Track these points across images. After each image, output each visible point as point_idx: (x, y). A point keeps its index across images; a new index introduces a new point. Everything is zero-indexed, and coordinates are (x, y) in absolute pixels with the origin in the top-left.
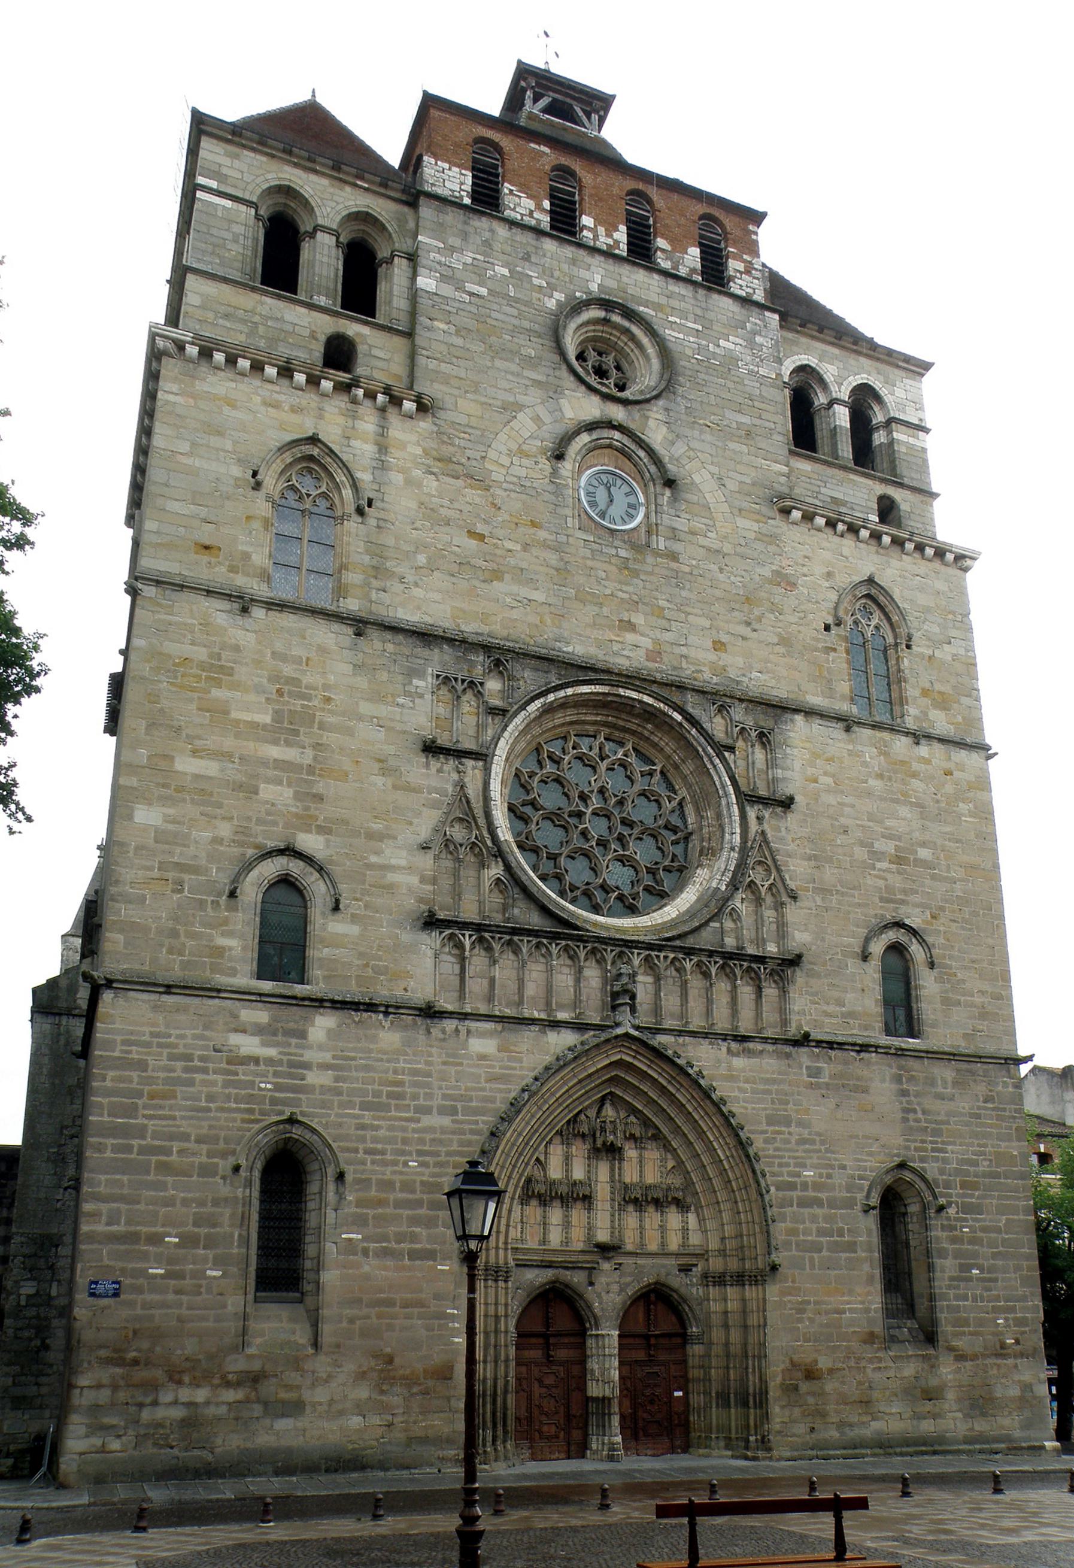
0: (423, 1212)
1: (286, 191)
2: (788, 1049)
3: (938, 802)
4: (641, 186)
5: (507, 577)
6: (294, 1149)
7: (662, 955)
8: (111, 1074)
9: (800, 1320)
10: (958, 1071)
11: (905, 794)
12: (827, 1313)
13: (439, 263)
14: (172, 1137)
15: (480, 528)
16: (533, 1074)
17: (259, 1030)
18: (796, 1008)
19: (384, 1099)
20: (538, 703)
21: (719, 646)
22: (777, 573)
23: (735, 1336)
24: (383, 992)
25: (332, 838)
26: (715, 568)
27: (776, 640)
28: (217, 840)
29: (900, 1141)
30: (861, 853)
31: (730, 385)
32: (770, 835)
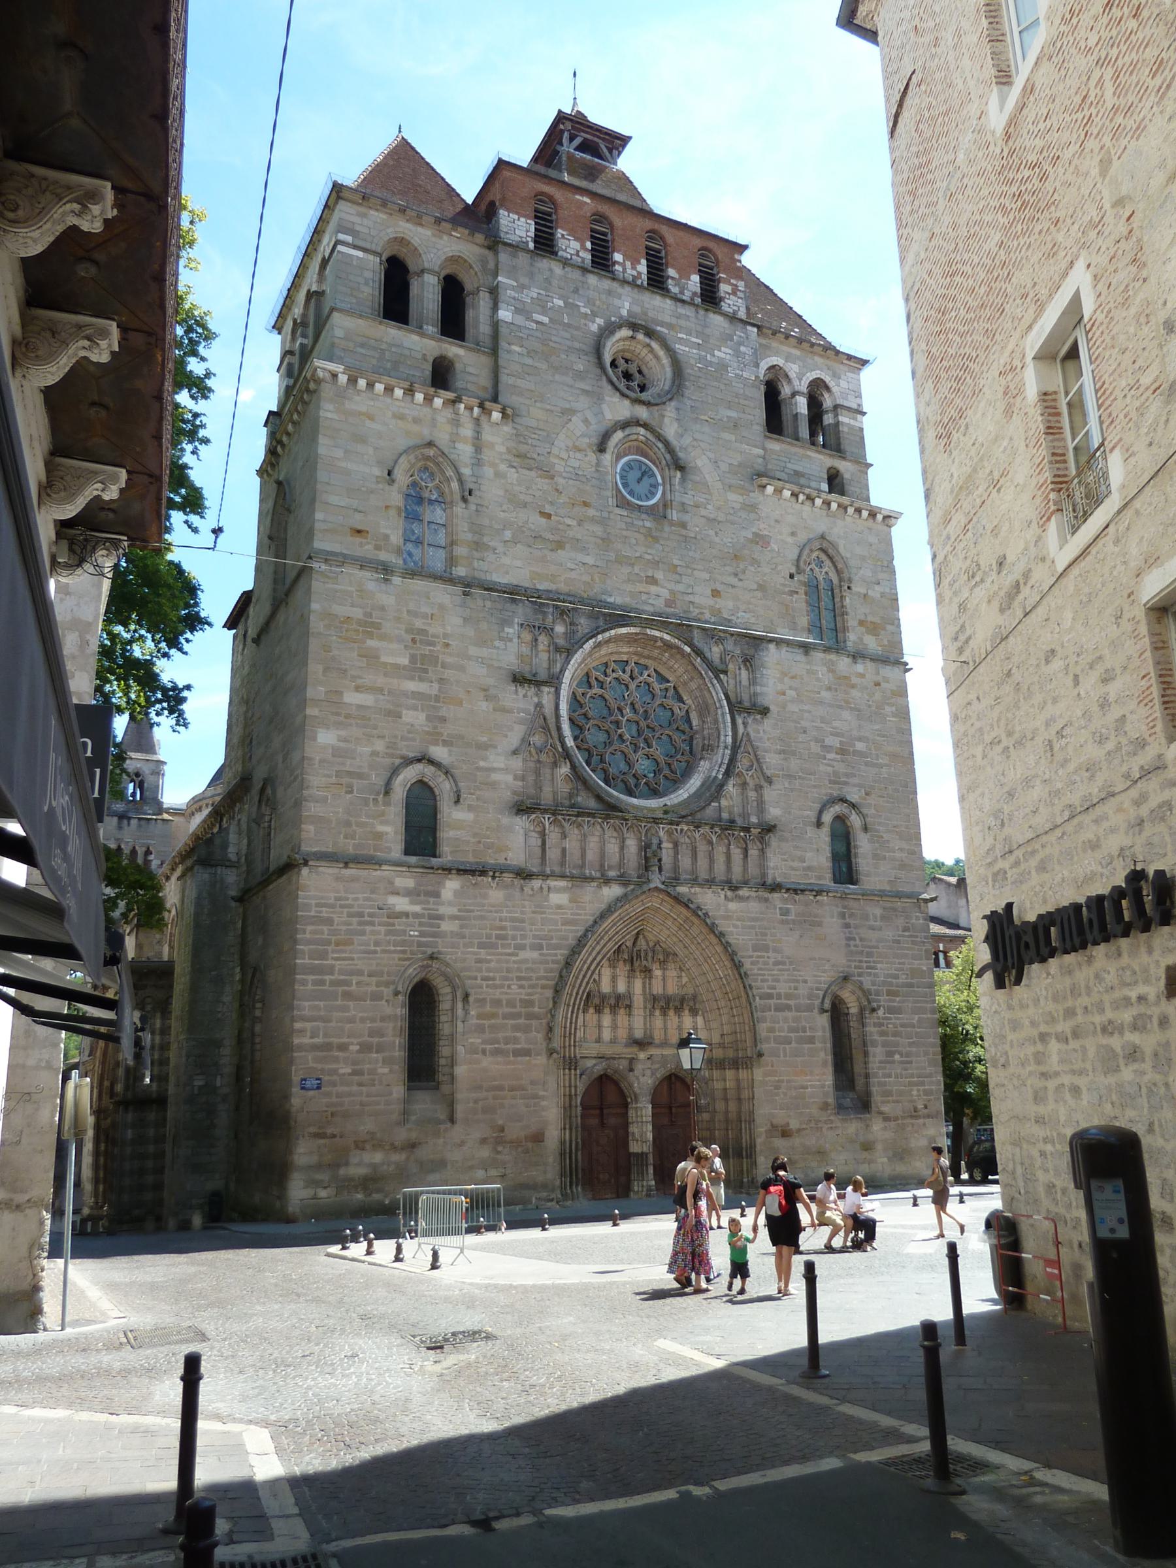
0: (522, 1021)
1: (401, 241)
2: (766, 895)
3: (870, 706)
4: (656, 226)
5: (568, 546)
6: (432, 978)
7: (679, 828)
8: (309, 928)
9: (777, 1094)
10: (884, 908)
11: (847, 702)
12: (795, 1088)
13: (514, 298)
14: (352, 973)
15: (548, 509)
16: (592, 918)
17: (408, 893)
18: (771, 864)
19: (493, 940)
20: (591, 642)
21: (716, 593)
22: (756, 534)
23: (732, 1106)
24: (491, 859)
25: (454, 749)
26: (712, 533)
27: (755, 587)
28: (374, 754)
30: (815, 748)
31: (723, 387)
32: (752, 734)
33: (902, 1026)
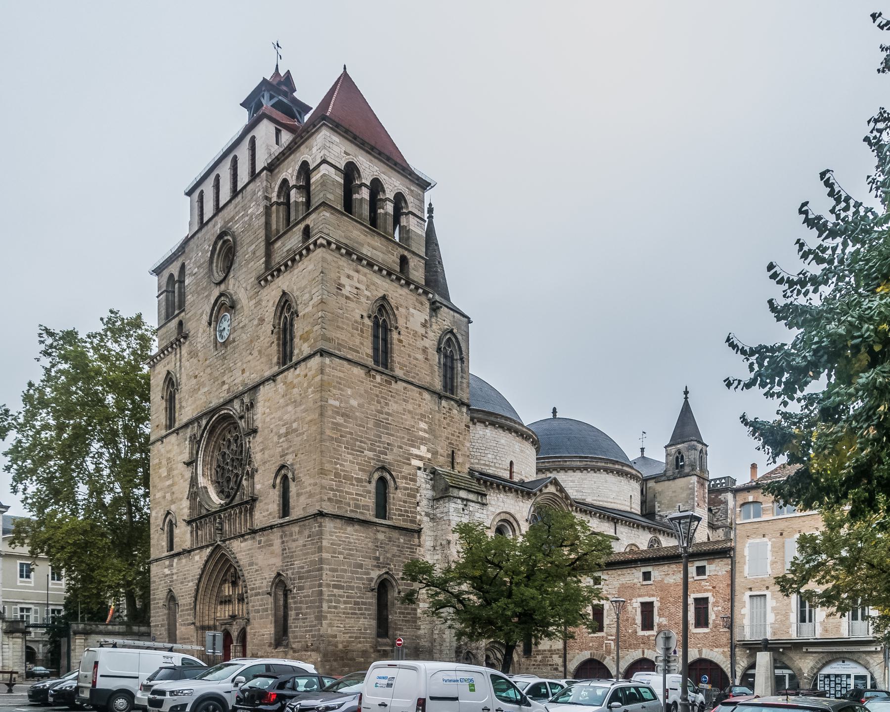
29: (281, 564)
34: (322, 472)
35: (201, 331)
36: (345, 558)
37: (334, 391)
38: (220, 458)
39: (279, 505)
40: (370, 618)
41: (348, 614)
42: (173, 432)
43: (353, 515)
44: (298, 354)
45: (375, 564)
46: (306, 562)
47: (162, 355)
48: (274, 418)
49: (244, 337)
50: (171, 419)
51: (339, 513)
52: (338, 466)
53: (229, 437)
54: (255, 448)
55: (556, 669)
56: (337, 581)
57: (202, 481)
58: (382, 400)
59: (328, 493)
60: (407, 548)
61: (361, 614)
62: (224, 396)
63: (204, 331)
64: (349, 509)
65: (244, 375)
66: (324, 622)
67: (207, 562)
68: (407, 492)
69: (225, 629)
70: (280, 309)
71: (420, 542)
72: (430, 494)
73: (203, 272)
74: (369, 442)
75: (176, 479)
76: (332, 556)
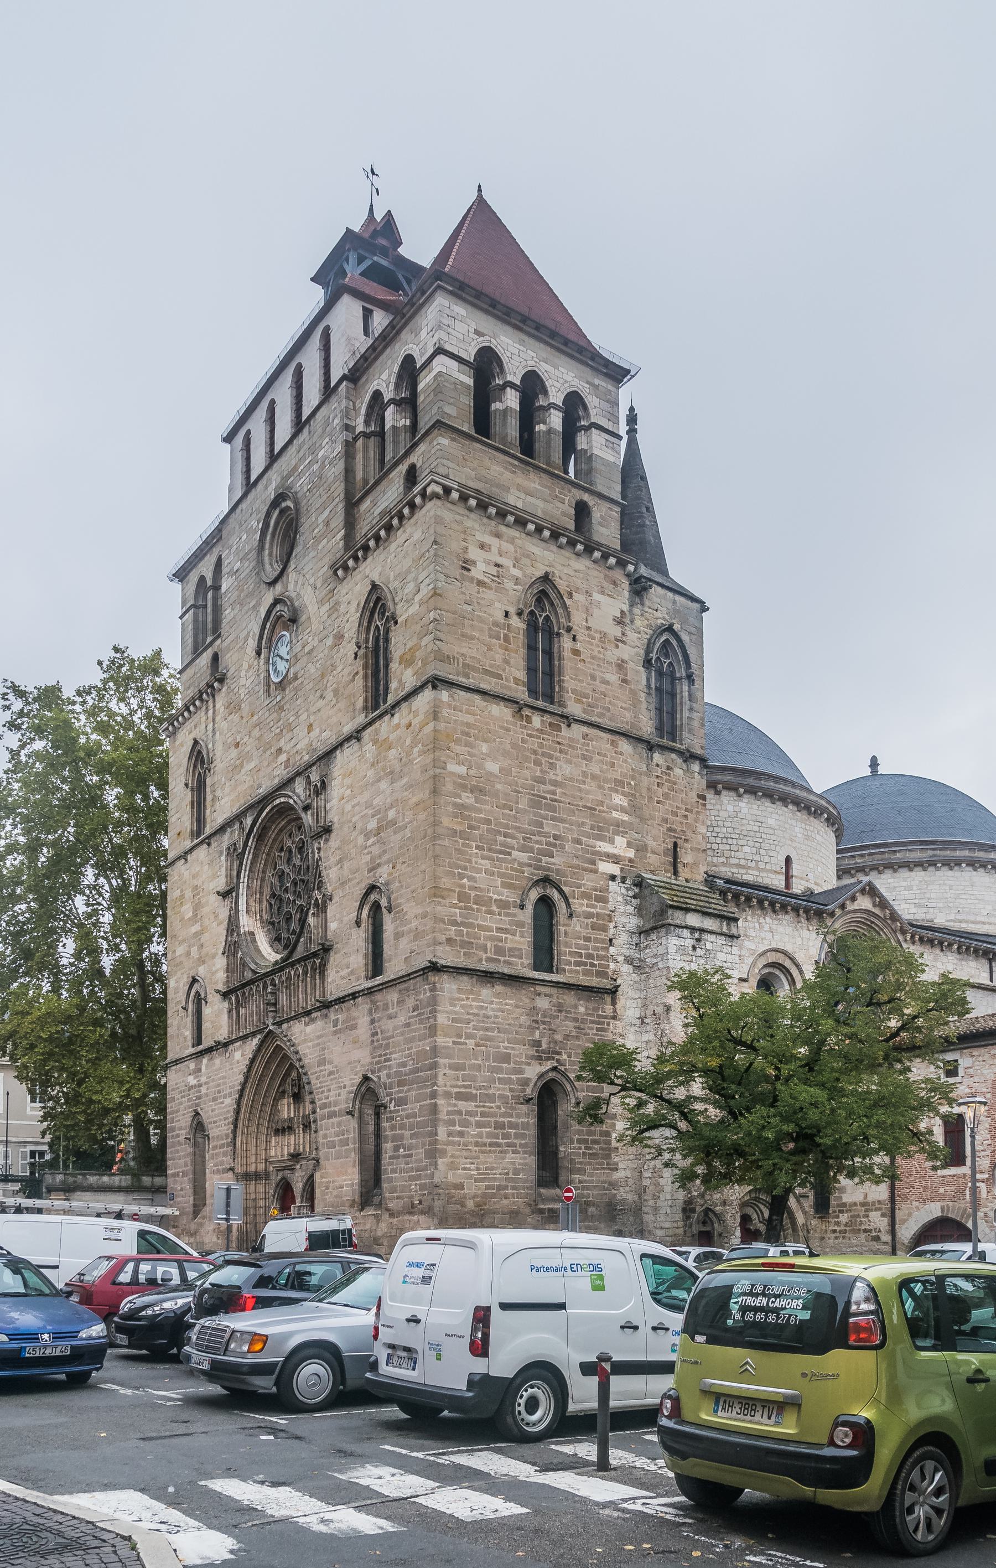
33: (408, 1117)
34: (437, 893)
35: (245, 666)
36: (477, 1045)
37: (458, 749)
38: (275, 881)
39: (366, 955)
40: (525, 1152)
41: (485, 1145)
42: (202, 843)
43: (492, 967)
44: (396, 689)
45: (534, 1053)
46: (410, 1055)
47: (186, 714)
48: (358, 804)
49: (312, 669)
50: (200, 820)
51: (467, 964)
52: (465, 880)
53: (289, 844)
54: (327, 858)
55: (877, 1239)
56: (465, 1086)
57: (247, 923)
58: (543, 760)
59: (446, 930)
60: (592, 1022)
61: (508, 1145)
62: (281, 773)
63: (250, 667)
64: (484, 956)
65: (311, 734)
66: (440, 1161)
67: (253, 1061)
68: (590, 921)
69: (283, 1178)
70: (368, 614)
71: (615, 1011)
72: (633, 922)
73: (249, 565)
74: (520, 836)
75: (206, 922)
76: (454, 1043)
